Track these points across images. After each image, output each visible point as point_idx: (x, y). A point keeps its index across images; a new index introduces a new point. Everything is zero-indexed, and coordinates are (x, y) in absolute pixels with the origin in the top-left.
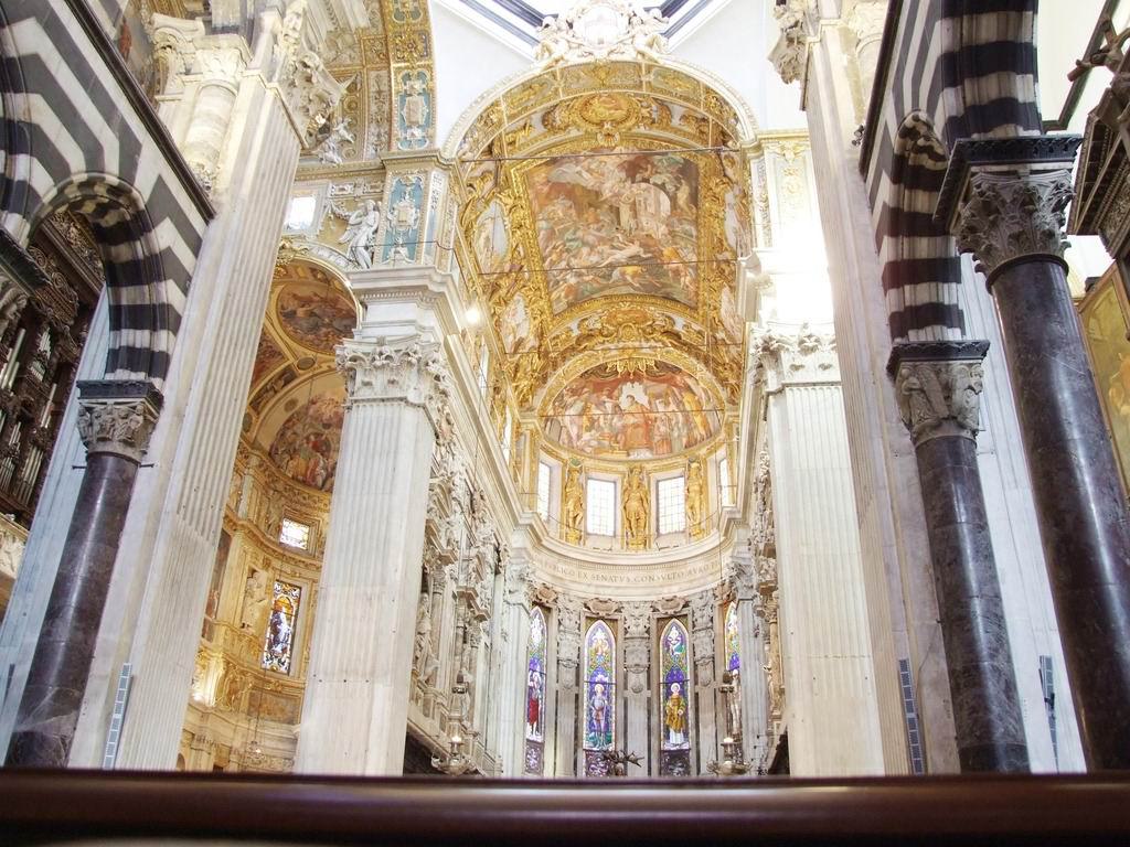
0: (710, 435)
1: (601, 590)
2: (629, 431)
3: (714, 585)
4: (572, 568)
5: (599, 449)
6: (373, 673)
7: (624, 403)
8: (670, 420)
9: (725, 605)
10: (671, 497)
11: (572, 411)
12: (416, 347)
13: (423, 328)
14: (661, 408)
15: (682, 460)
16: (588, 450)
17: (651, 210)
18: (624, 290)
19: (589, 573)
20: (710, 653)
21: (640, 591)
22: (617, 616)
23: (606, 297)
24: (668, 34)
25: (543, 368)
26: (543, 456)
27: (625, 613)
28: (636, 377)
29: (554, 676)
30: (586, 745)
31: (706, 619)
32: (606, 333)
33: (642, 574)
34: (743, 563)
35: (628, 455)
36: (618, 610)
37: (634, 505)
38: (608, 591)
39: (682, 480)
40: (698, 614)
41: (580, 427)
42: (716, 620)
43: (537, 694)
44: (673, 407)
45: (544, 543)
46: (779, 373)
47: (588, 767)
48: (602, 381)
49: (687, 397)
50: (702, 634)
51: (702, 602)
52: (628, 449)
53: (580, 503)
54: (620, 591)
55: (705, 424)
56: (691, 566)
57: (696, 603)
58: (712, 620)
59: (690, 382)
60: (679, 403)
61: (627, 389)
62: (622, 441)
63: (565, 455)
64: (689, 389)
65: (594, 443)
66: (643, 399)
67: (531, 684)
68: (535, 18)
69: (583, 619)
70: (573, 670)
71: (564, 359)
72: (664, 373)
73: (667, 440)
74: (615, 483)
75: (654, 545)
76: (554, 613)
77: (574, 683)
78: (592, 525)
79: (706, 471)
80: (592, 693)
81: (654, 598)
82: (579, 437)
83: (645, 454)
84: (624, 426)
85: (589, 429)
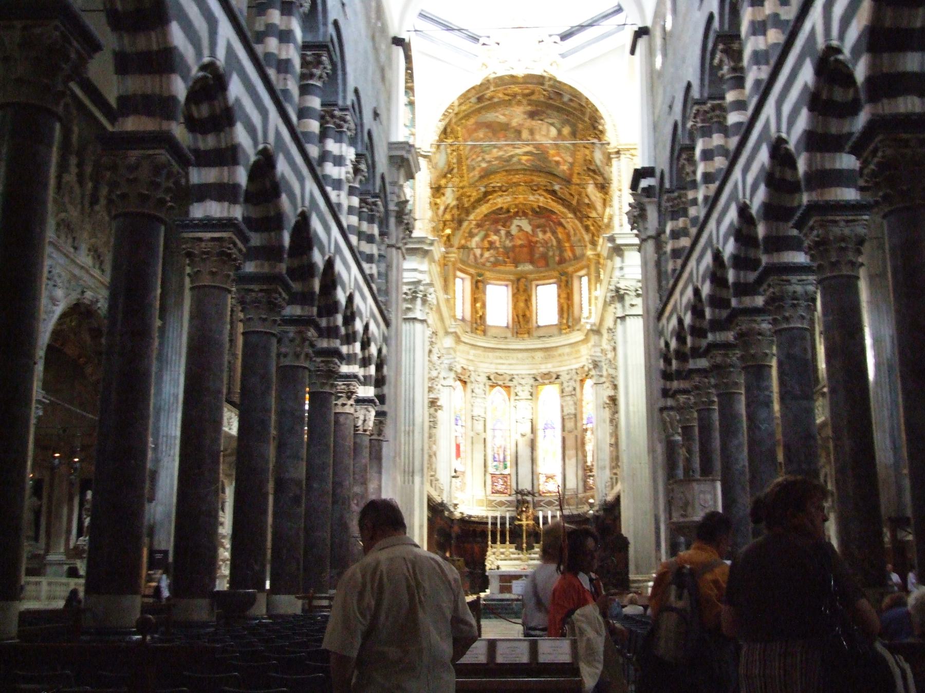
0: (576, 258)
1: (499, 366)
2: (517, 250)
3: (577, 366)
4: (479, 352)
5: (495, 264)
6: (413, 472)
7: (514, 230)
8: (546, 243)
9: (582, 381)
10: (546, 298)
11: (477, 239)
12: (421, 288)
13: (421, 272)
14: (540, 235)
15: (556, 274)
16: (488, 264)
17: (544, 133)
18: (519, 167)
19: (491, 354)
20: (573, 411)
21: (526, 367)
22: (510, 384)
23: (506, 171)
24: (563, 56)
25: (459, 215)
26: (459, 274)
27: (515, 382)
28: (525, 214)
29: (470, 427)
30: (491, 470)
31: (571, 389)
32: (504, 189)
33: (525, 354)
34: (597, 359)
35: (516, 267)
36: (511, 380)
37: (522, 304)
38: (504, 367)
39: (555, 287)
40: (565, 384)
41: (482, 249)
42: (578, 389)
43: (461, 441)
44: (549, 234)
45: (463, 339)
46: (623, 306)
47: (493, 485)
48: (500, 218)
49: (560, 230)
50: (568, 398)
51: (568, 377)
52: (516, 263)
53: (484, 306)
54: (512, 367)
55: (573, 251)
56: (560, 351)
57: (564, 377)
58: (575, 389)
59: (562, 220)
60: (554, 233)
61: (516, 222)
62: (513, 255)
63: (472, 271)
64: (561, 224)
65: (492, 259)
66: (528, 228)
67: (457, 434)
68: (476, 39)
69: (487, 387)
70: (482, 423)
71: (474, 208)
72: (541, 214)
73: (545, 257)
74: (507, 286)
75: (535, 334)
76: (469, 385)
77: (482, 430)
78: (491, 320)
79: (572, 284)
80: (494, 437)
81: (534, 372)
82: (482, 255)
83: (528, 267)
84: (514, 247)
85: (488, 249)
